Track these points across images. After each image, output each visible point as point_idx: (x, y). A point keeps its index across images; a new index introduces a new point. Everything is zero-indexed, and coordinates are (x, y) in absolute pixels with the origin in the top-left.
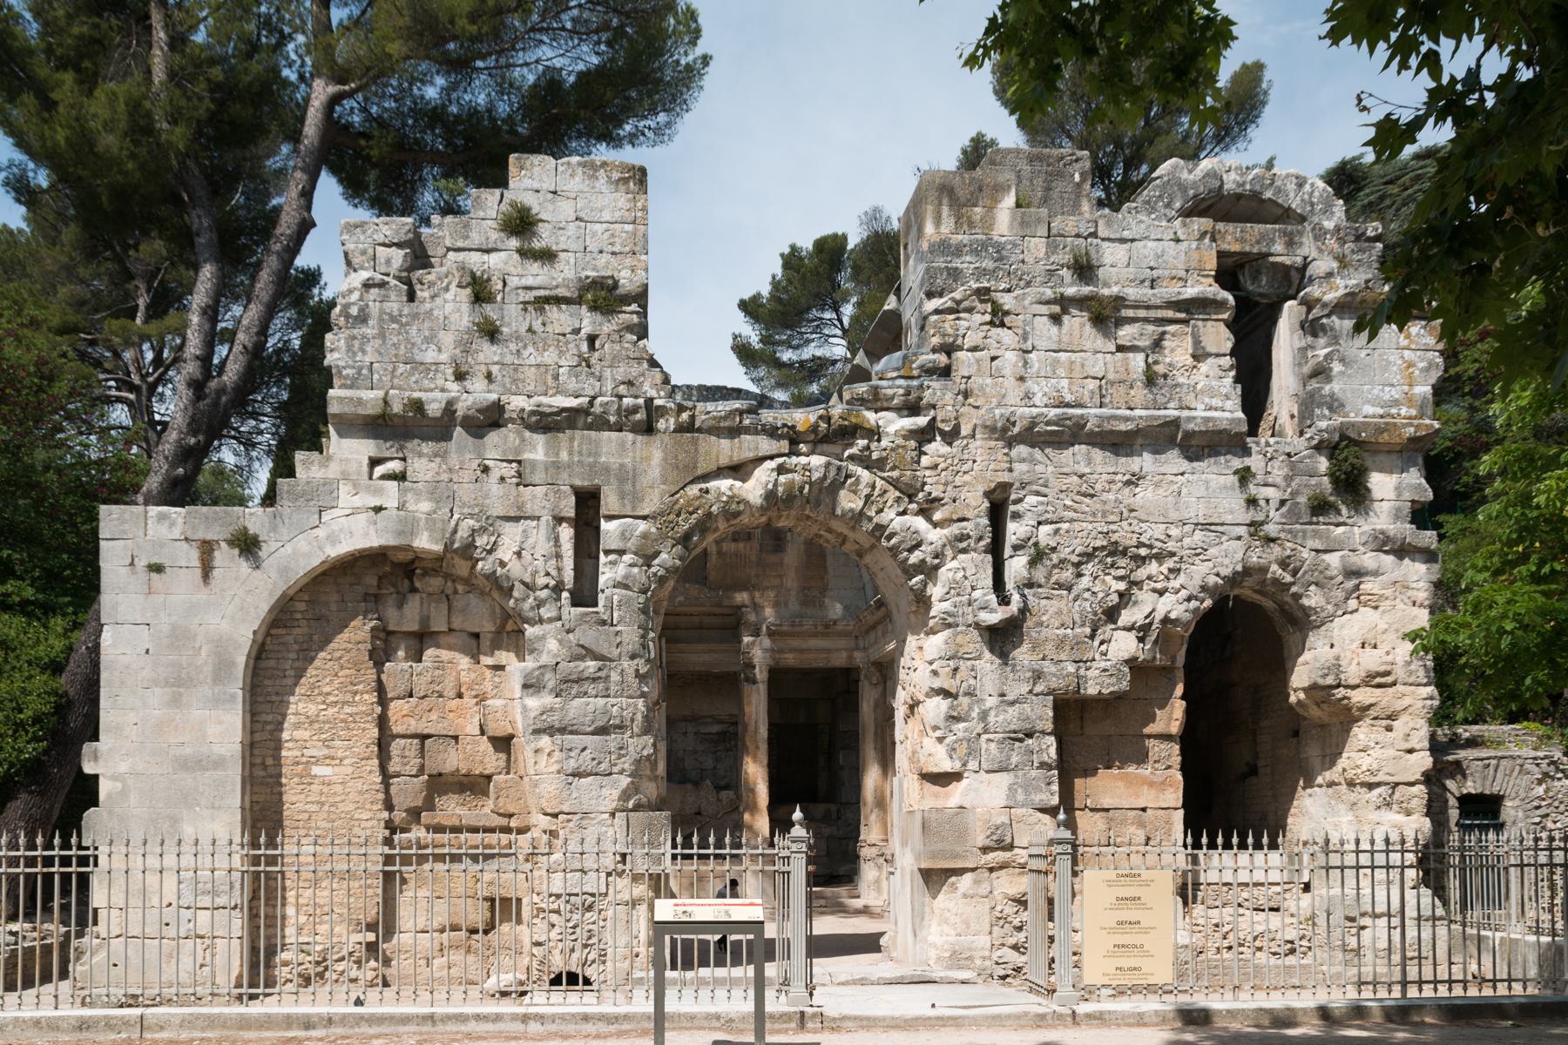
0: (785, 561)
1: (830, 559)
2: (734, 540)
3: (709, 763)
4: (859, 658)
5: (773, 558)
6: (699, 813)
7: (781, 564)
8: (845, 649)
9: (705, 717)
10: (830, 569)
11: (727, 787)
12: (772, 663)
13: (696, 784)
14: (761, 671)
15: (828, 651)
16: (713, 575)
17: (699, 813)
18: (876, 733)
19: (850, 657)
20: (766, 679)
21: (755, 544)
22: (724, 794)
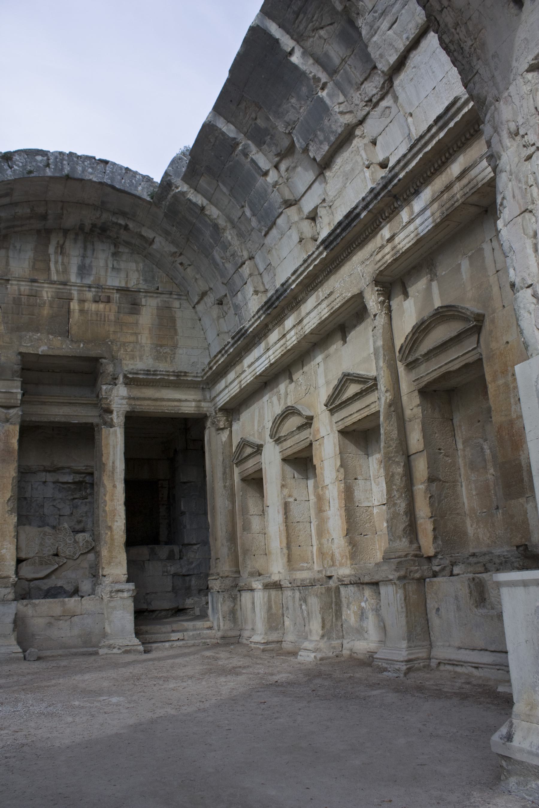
0: (140, 322)
1: (179, 323)
2: (96, 301)
3: (67, 511)
4: (206, 407)
5: (130, 319)
6: (57, 555)
7: (137, 323)
8: (194, 400)
9: (63, 468)
10: (179, 331)
11: (83, 531)
12: (128, 409)
13: (54, 527)
14: (118, 417)
15: (180, 400)
16: (74, 330)
17: (57, 555)
18: (224, 473)
19: (198, 407)
20: (122, 423)
21: (114, 307)
22: (80, 537)
